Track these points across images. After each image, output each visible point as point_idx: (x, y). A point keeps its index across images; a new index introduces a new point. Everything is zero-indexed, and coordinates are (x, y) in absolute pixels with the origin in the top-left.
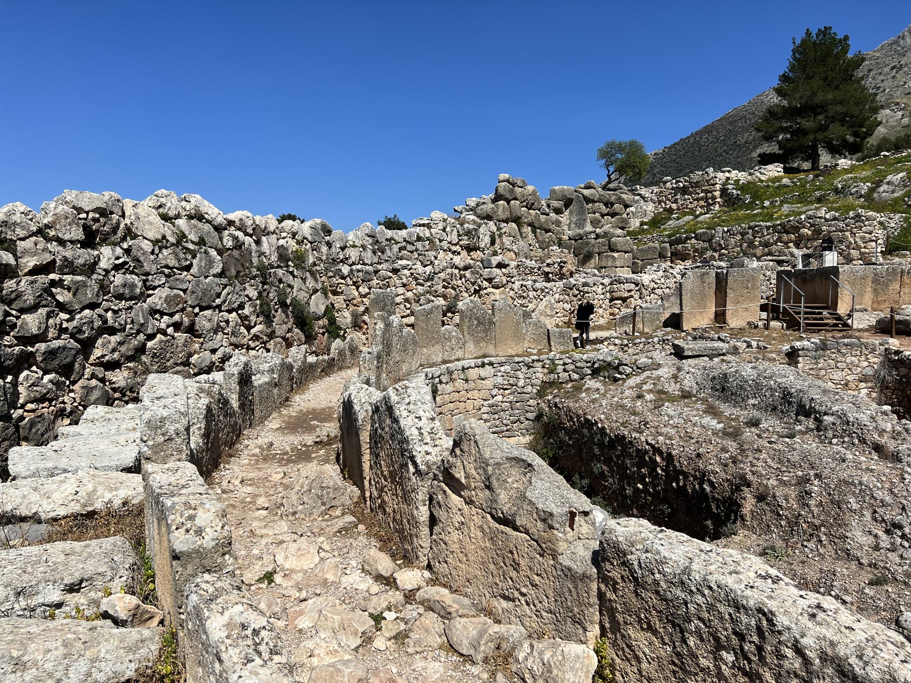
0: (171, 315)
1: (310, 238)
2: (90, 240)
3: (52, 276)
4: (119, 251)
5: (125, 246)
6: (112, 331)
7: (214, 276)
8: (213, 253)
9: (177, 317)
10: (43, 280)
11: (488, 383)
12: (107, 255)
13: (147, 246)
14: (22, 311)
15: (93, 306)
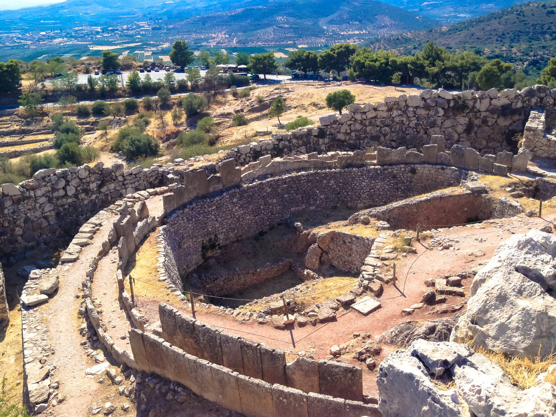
0: (416, 129)
1: (523, 95)
2: (390, 110)
3: (376, 119)
4: (399, 112)
5: (403, 109)
6: (394, 132)
7: (439, 117)
8: (440, 110)
9: (418, 130)
10: (373, 120)
11: (449, 176)
12: (395, 113)
13: (411, 109)
14: (366, 127)
15: (387, 126)
